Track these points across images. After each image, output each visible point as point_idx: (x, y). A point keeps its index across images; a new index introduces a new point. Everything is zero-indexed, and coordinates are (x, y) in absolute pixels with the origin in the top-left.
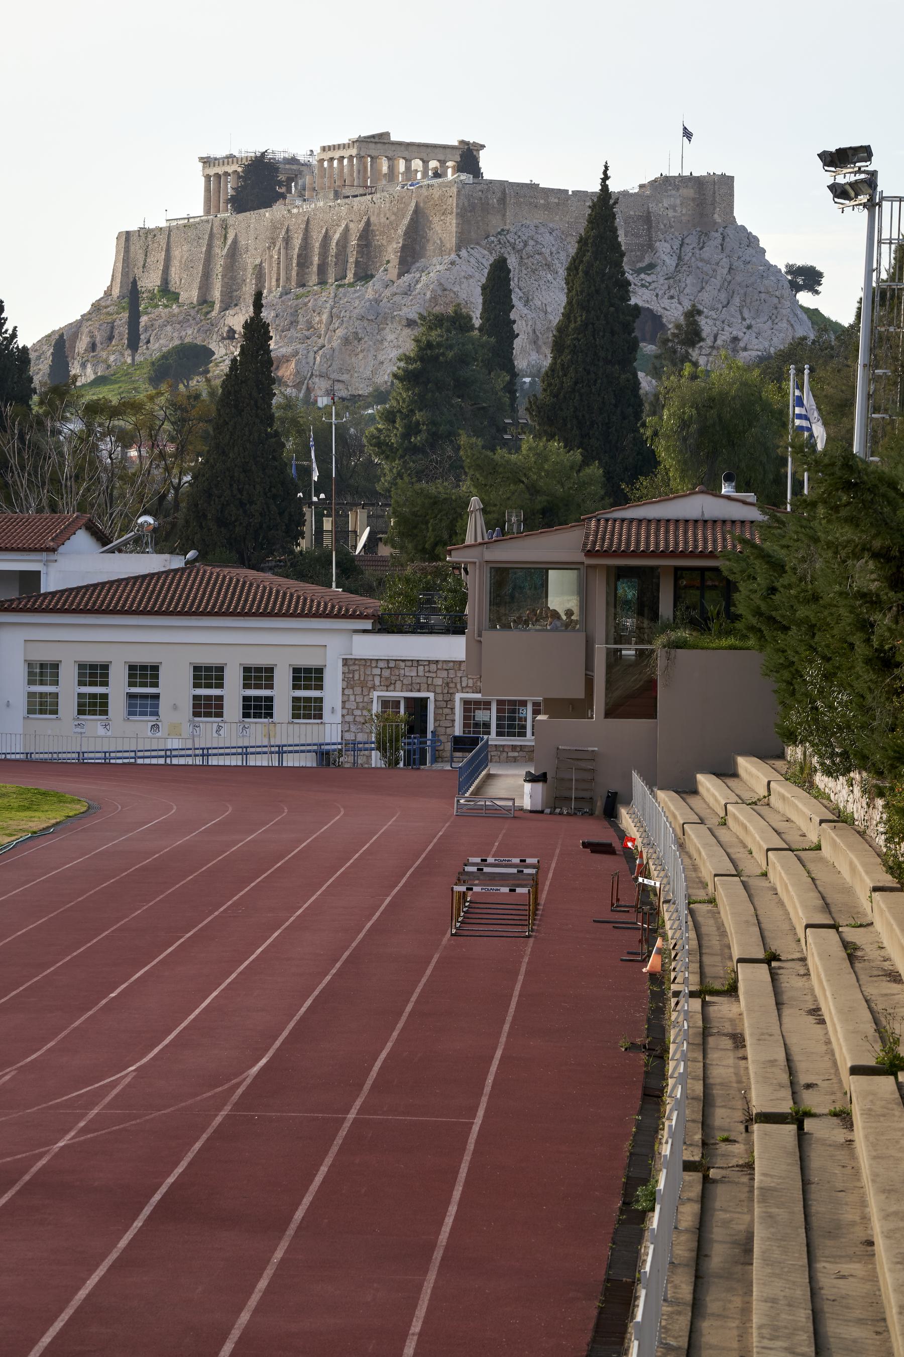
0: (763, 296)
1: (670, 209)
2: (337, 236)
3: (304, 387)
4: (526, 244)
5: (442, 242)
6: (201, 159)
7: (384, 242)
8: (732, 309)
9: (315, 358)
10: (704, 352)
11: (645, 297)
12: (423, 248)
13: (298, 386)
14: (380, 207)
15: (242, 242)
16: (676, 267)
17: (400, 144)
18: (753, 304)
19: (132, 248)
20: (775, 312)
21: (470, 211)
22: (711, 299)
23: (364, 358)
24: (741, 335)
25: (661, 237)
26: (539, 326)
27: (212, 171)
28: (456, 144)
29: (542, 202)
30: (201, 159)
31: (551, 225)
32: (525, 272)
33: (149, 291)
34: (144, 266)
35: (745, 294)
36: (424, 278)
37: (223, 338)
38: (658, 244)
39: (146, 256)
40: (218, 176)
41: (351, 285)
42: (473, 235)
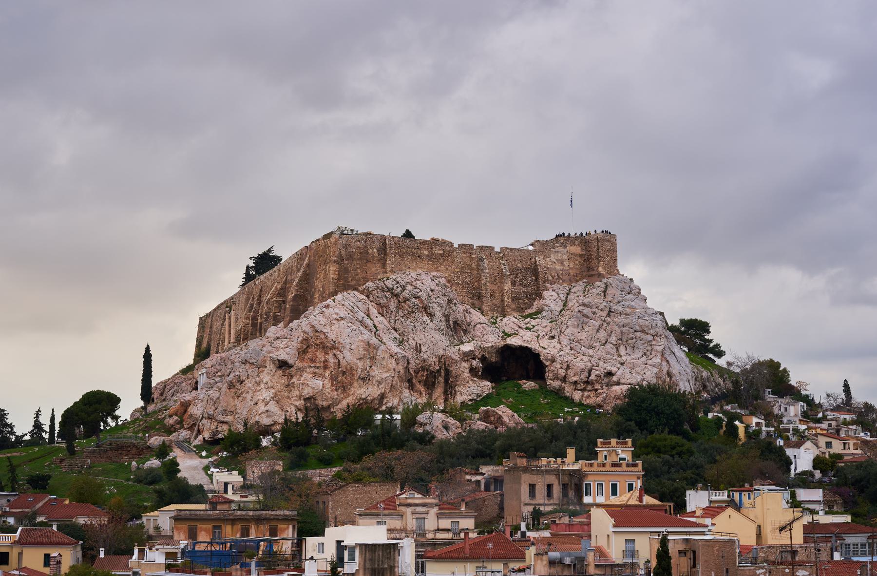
0: (638, 334)
3: (196, 429)
4: (404, 288)
8: (608, 346)
10: (579, 386)
11: (525, 338)
12: (312, 297)
13: (191, 428)
16: (561, 311)
18: (629, 342)
20: (649, 348)
21: (348, 259)
22: (589, 338)
24: (614, 369)
25: (549, 285)
26: (412, 365)
31: (435, 273)
38: (545, 293)
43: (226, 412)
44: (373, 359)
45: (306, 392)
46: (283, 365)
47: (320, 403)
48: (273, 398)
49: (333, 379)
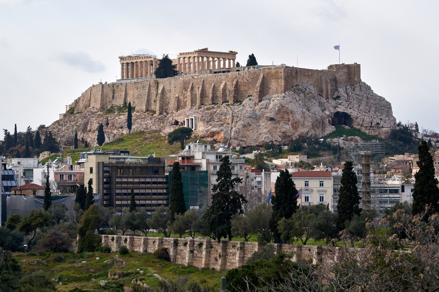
0: (383, 107)
1: (341, 76)
2: (222, 86)
3: (228, 143)
4: (306, 90)
5: (277, 89)
6: (120, 58)
7: (246, 89)
9: (231, 132)
10: (368, 128)
14: (243, 76)
15: (167, 88)
17: (211, 52)
19: (105, 91)
23: (253, 132)
24: (380, 122)
27: (125, 62)
28: (227, 52)
30: (120, 58)
32: (307, 100)
33: (118, 106)
34: (113, 97)
35: (376, 107)
37: (172, 124)
38: (339, 89)
39: (114, 93)
40: (128, 64)
42: (289, 87)
43: (243, 137)
44: (304, 118)
45: (283, 130)
46: (272, 119)
47: (288, 134)
48: (268, 132)
49: (292, 125)
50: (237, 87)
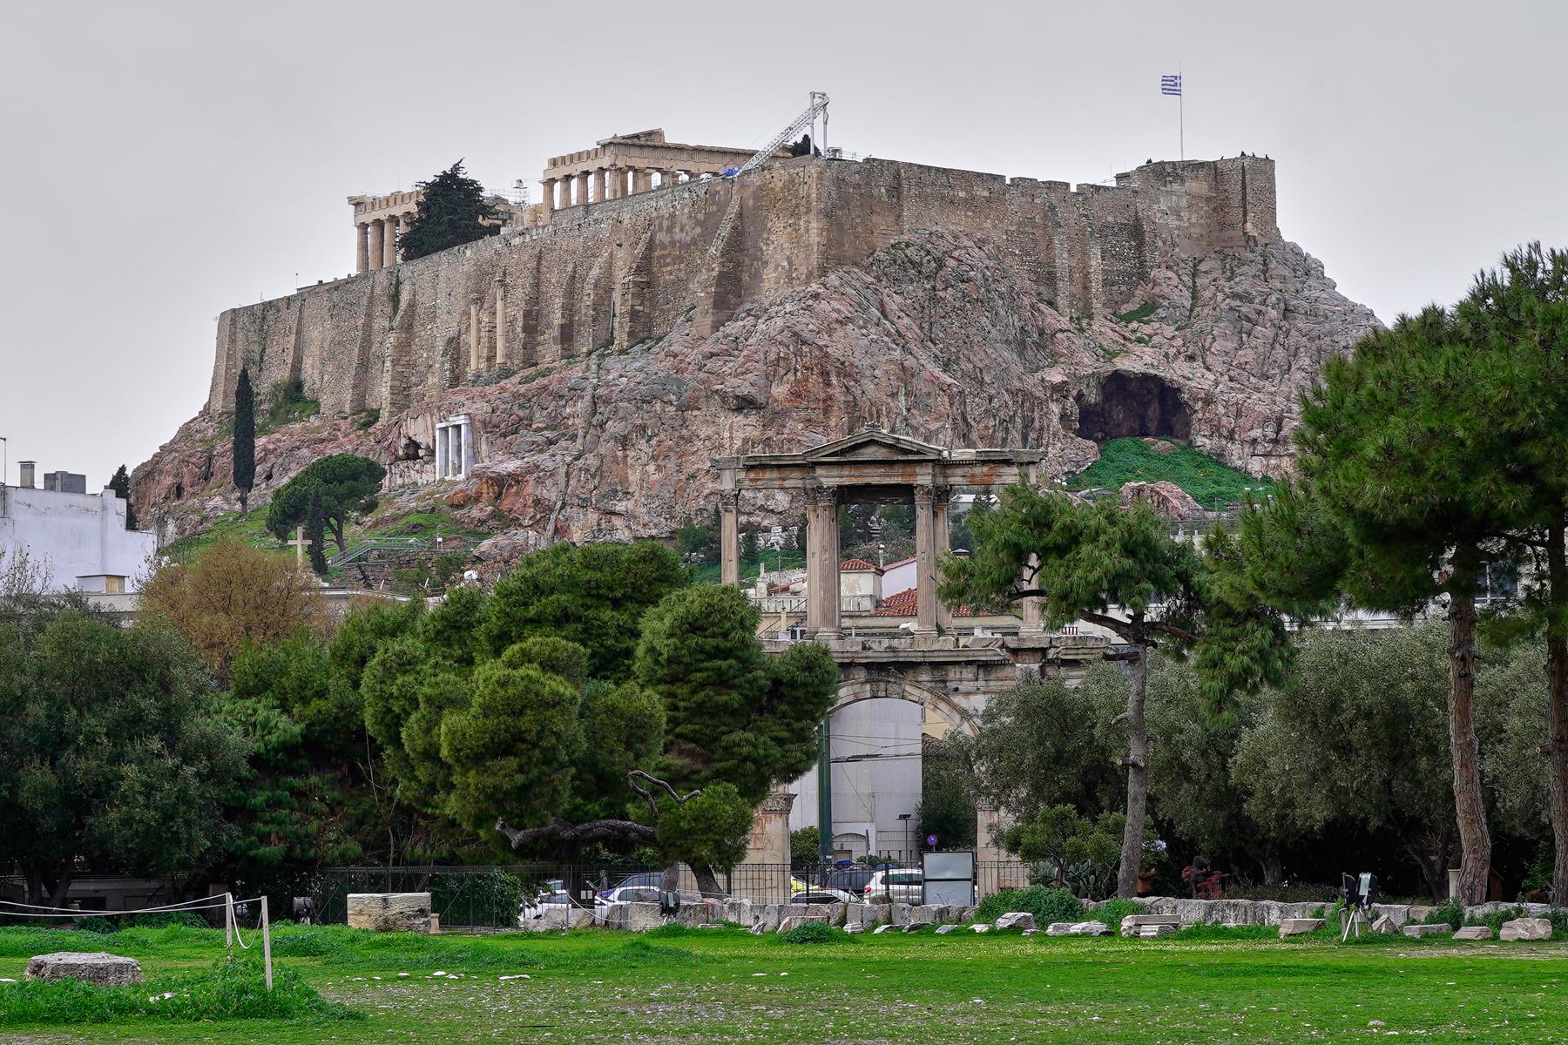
2: (595, 272)
5: (790, 263)
7: (682, 275)
29: (962, 194)
36: (761, 327)
41: (623, 352)
50: (645, 265)
